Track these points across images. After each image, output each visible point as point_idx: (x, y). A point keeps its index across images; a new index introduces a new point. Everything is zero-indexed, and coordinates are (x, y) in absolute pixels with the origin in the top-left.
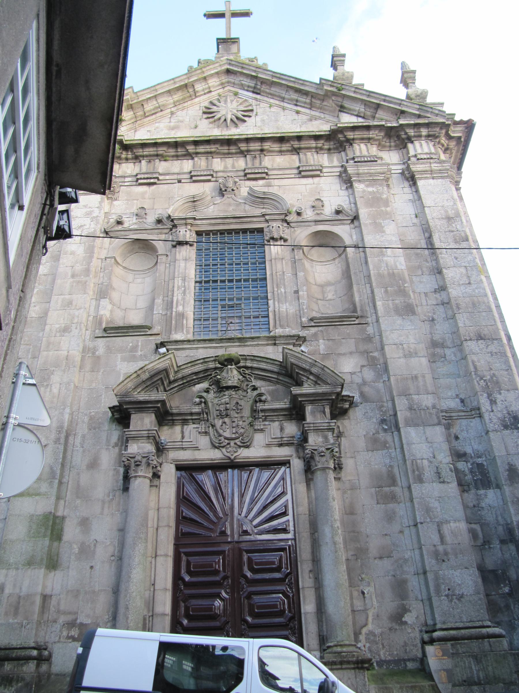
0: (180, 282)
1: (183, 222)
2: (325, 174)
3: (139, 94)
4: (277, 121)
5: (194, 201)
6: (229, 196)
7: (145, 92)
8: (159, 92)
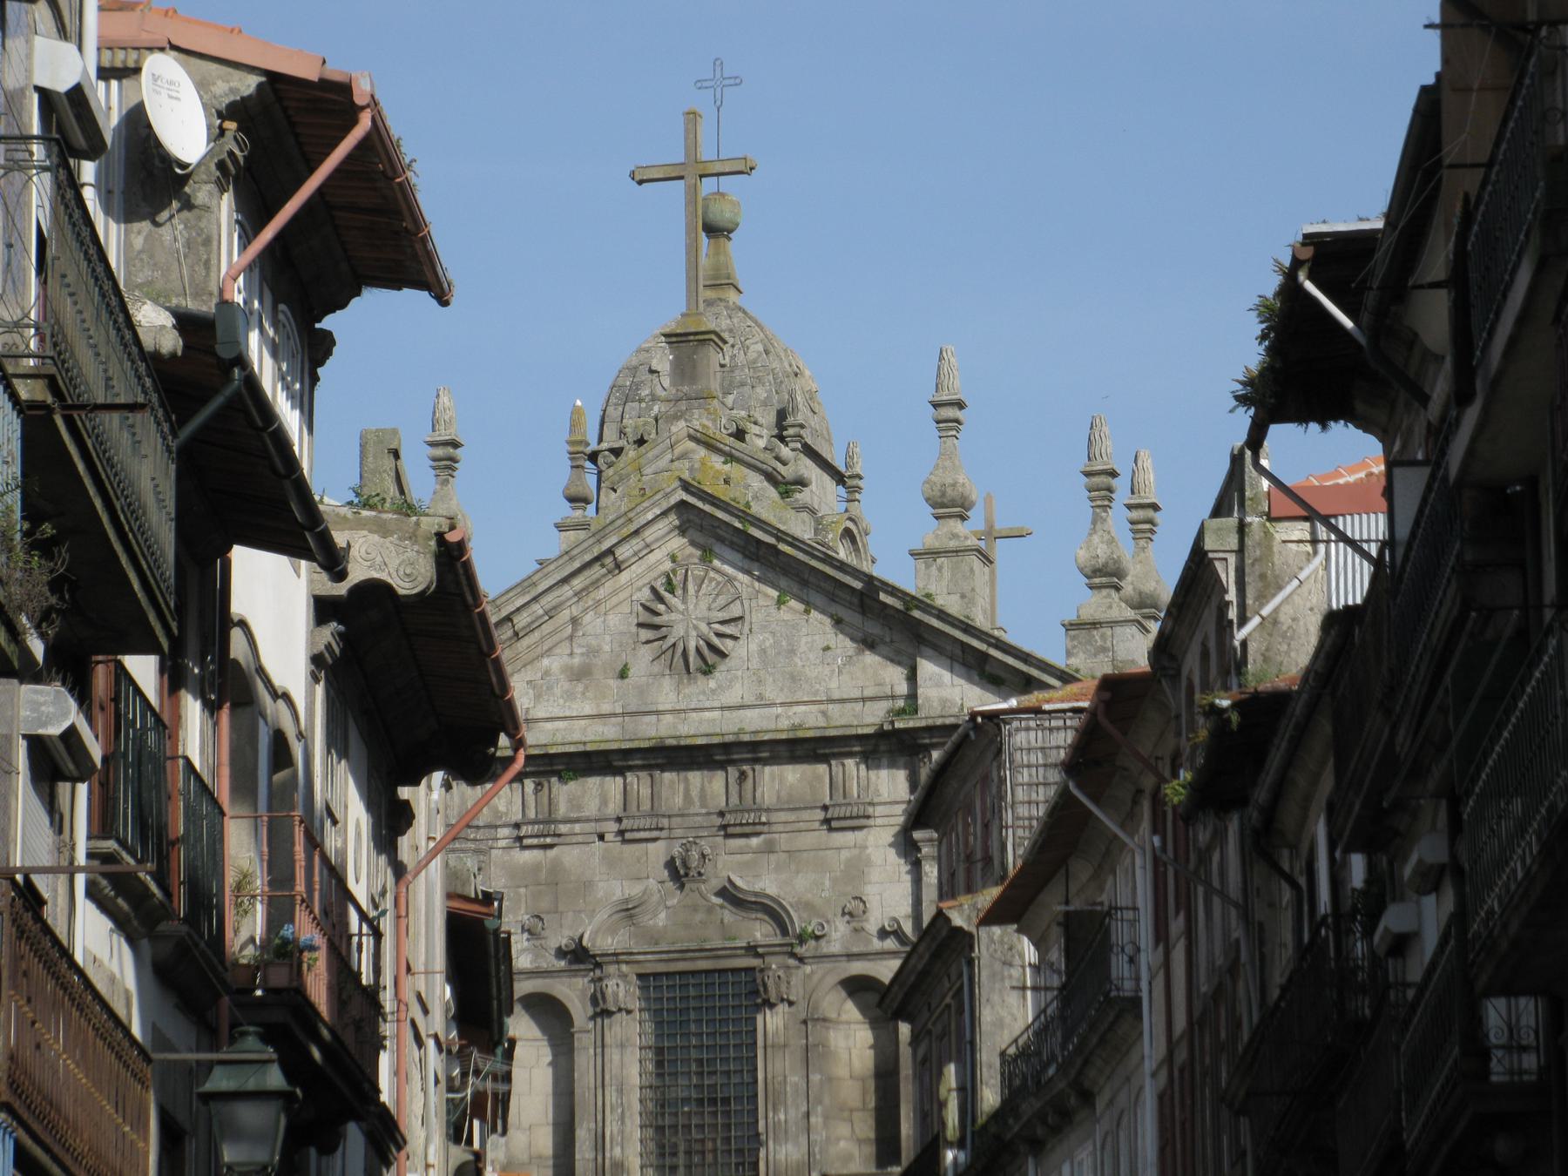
0: (614, 1094)
1: (611, 958)
2: (879, 821)
3: (498, 602)
4: (792, 652)
5: (628, 910)
6: (694, 886)
7: (511, 594)
8: (541, 588)
